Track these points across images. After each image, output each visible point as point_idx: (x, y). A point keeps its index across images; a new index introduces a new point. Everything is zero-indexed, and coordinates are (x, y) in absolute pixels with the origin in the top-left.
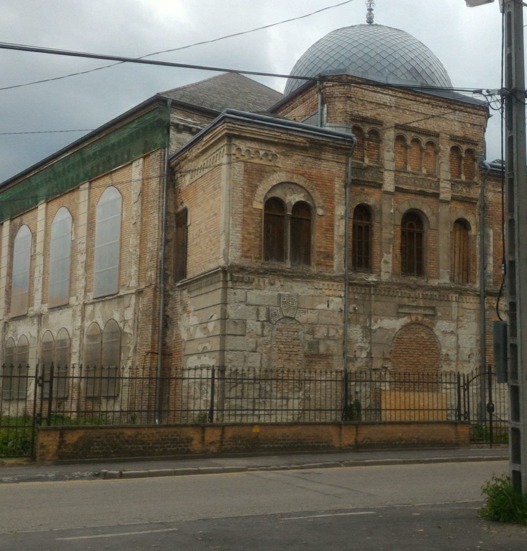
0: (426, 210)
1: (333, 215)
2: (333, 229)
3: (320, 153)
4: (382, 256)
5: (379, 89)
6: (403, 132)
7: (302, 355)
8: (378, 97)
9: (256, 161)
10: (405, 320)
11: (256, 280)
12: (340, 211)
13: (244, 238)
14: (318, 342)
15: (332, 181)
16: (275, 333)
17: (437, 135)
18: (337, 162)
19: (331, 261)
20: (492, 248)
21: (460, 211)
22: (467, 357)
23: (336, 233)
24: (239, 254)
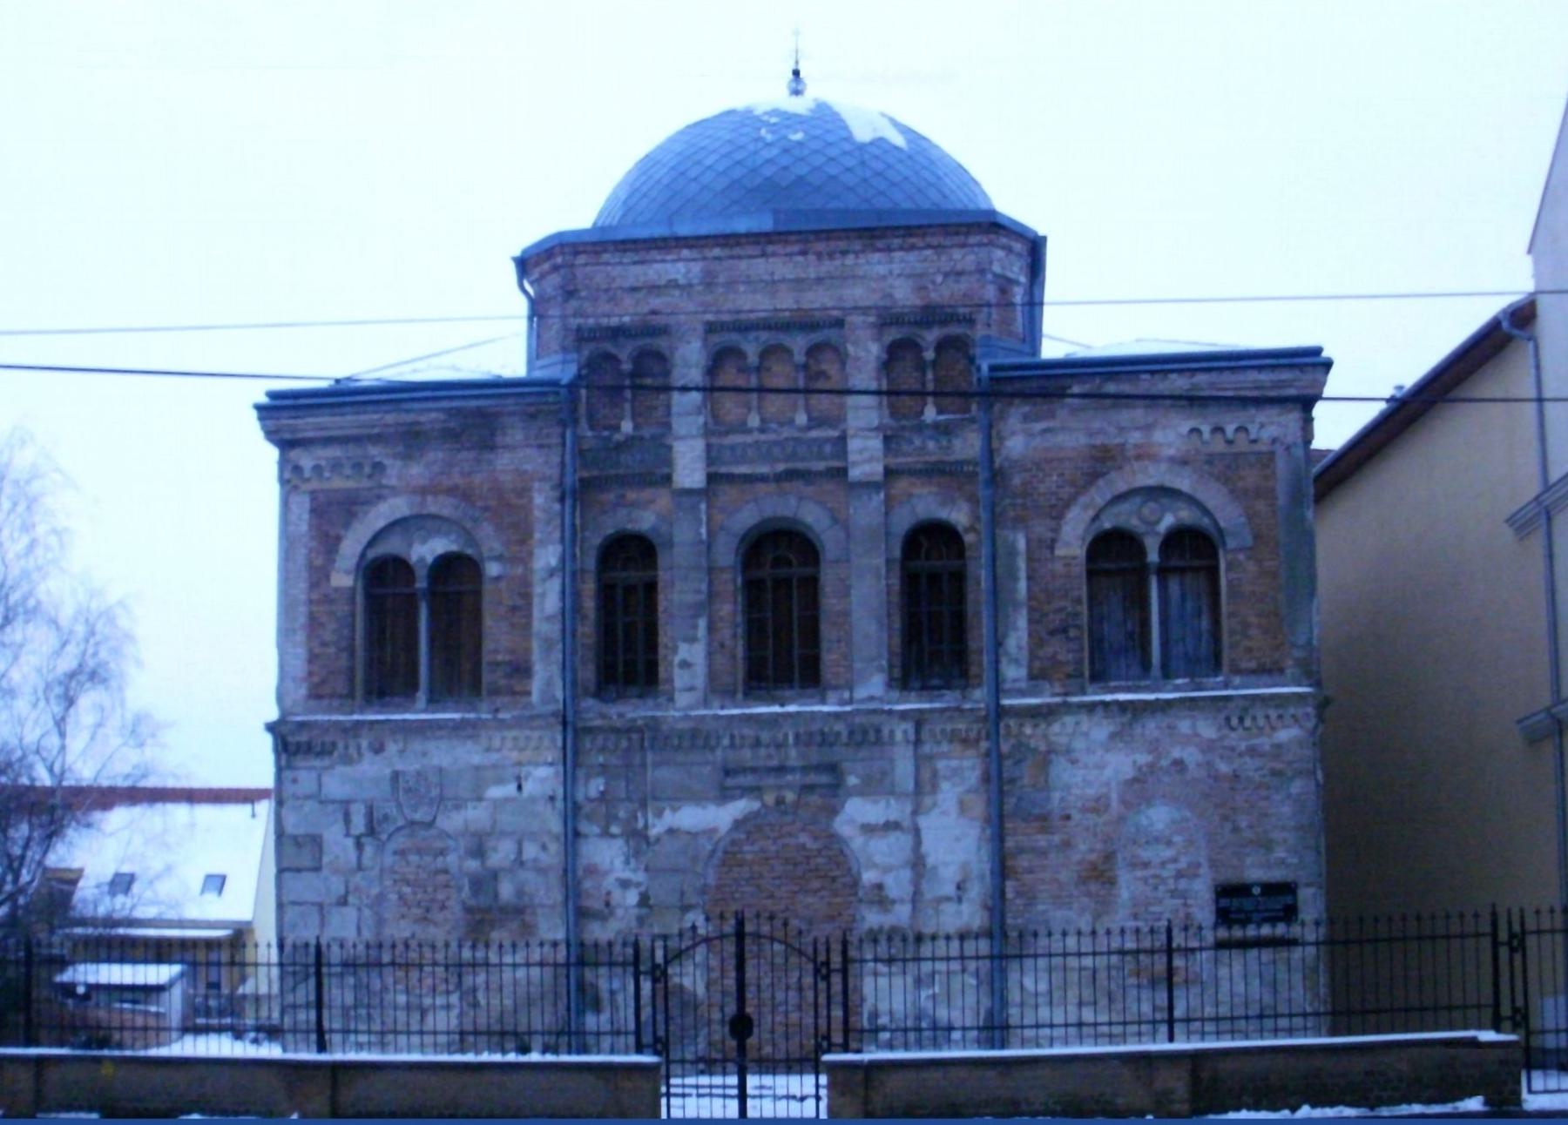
1: (529, 571)
2: (529, 605)
5: (655, 255)
9: (338, 483)
10: (740, 807)
11: (341, 745)
12: (547, 556)
13: (312, 658)
14: (495, 875)
15: (524, 492)
16: (389, 860)
23: (536, 613)
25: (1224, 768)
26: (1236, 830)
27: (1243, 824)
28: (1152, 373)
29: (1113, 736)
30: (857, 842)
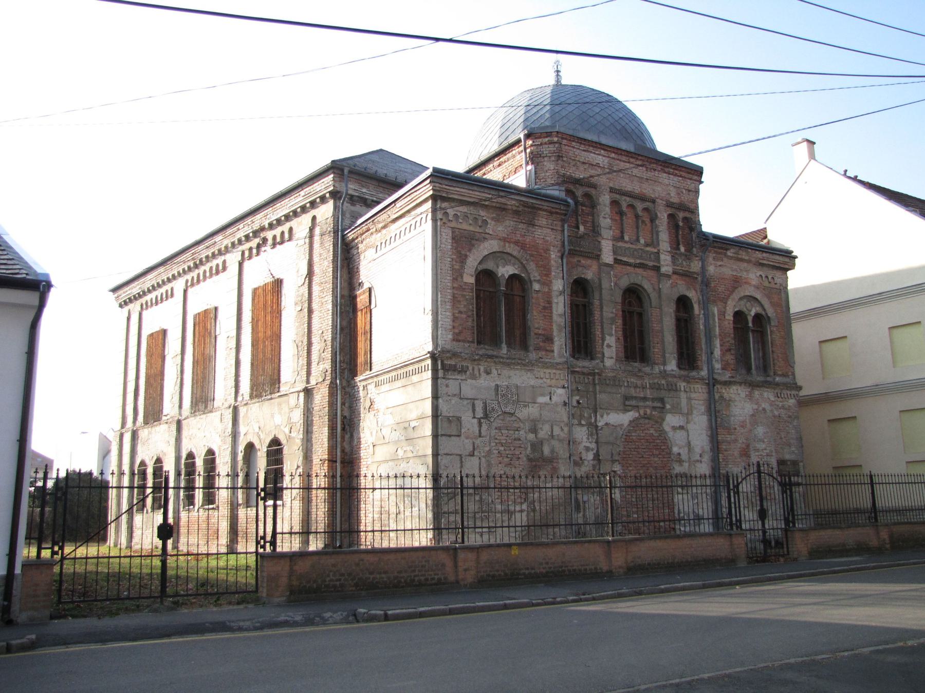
0: (647, 285)
1: (550, 291)
4: (603, 339)
6: (618, 196)
7: (525, 459)
8: (590, 157)
9: (465, 226)
10: (631, 415)
11: (470, 368)
12: (558, 285)
14: (541, 443)
15: (547, 250)
16: (494, 432)
17: (653, 201)
18: (552, 229)
19: (551, 345)
20: (717, 329)
21: (683, 289)
22: (699, 456)
23: (554, 312)
24: (450, 337)
26: (781, 438)
27: (783, 436)
30: (671, 434)
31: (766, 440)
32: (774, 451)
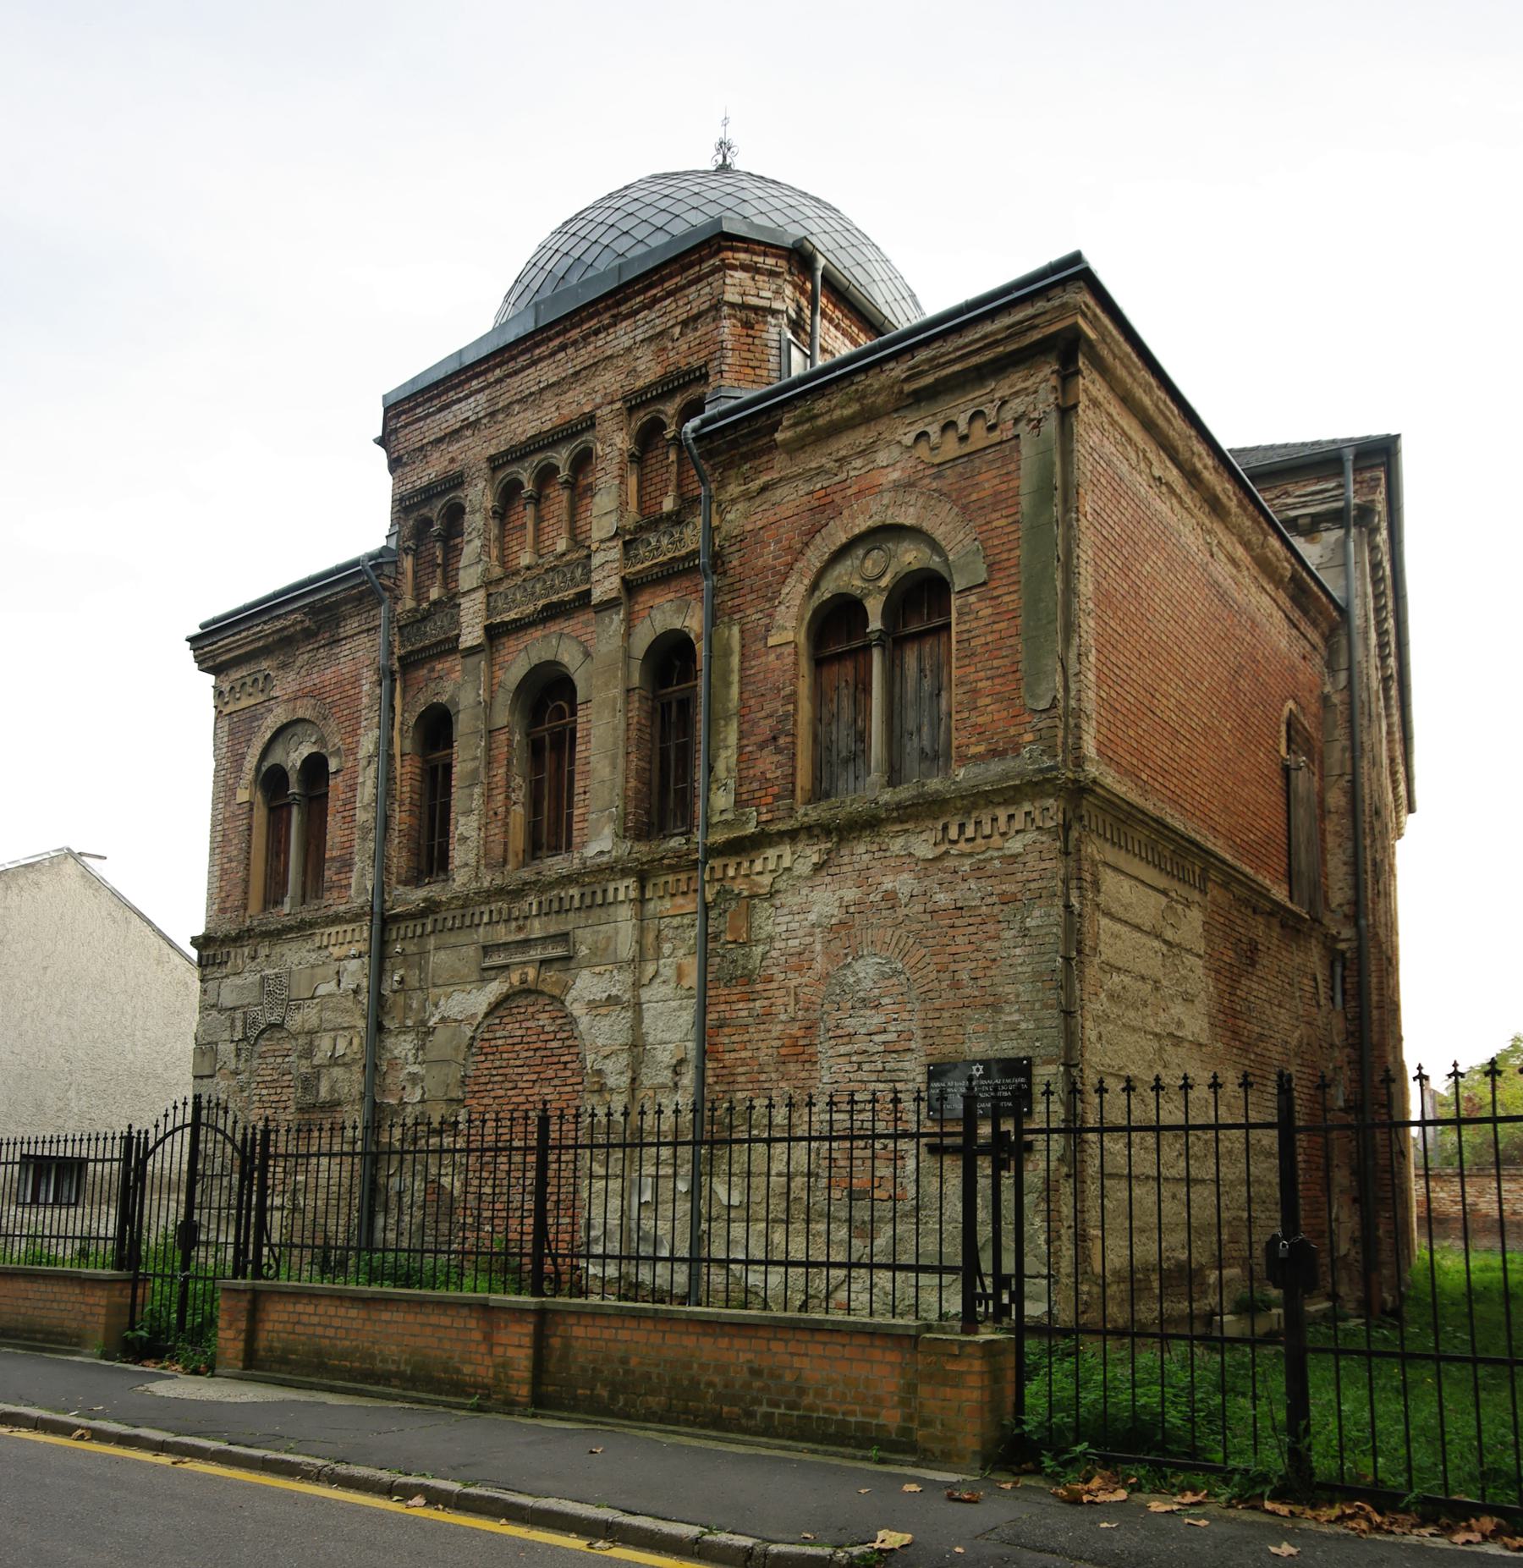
3: (338, 626)
6: (541, 456)
10: (495, 989)
18: (368, 630)
22: (668, 1073)
25: (942, 898)
26: (956, 985)
28: (865, 369)
29: (818, 868)
30: (584, 1022)
31: (885, 1001)
32: (919, 1033)
